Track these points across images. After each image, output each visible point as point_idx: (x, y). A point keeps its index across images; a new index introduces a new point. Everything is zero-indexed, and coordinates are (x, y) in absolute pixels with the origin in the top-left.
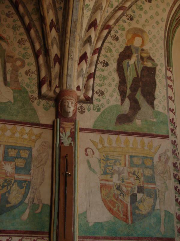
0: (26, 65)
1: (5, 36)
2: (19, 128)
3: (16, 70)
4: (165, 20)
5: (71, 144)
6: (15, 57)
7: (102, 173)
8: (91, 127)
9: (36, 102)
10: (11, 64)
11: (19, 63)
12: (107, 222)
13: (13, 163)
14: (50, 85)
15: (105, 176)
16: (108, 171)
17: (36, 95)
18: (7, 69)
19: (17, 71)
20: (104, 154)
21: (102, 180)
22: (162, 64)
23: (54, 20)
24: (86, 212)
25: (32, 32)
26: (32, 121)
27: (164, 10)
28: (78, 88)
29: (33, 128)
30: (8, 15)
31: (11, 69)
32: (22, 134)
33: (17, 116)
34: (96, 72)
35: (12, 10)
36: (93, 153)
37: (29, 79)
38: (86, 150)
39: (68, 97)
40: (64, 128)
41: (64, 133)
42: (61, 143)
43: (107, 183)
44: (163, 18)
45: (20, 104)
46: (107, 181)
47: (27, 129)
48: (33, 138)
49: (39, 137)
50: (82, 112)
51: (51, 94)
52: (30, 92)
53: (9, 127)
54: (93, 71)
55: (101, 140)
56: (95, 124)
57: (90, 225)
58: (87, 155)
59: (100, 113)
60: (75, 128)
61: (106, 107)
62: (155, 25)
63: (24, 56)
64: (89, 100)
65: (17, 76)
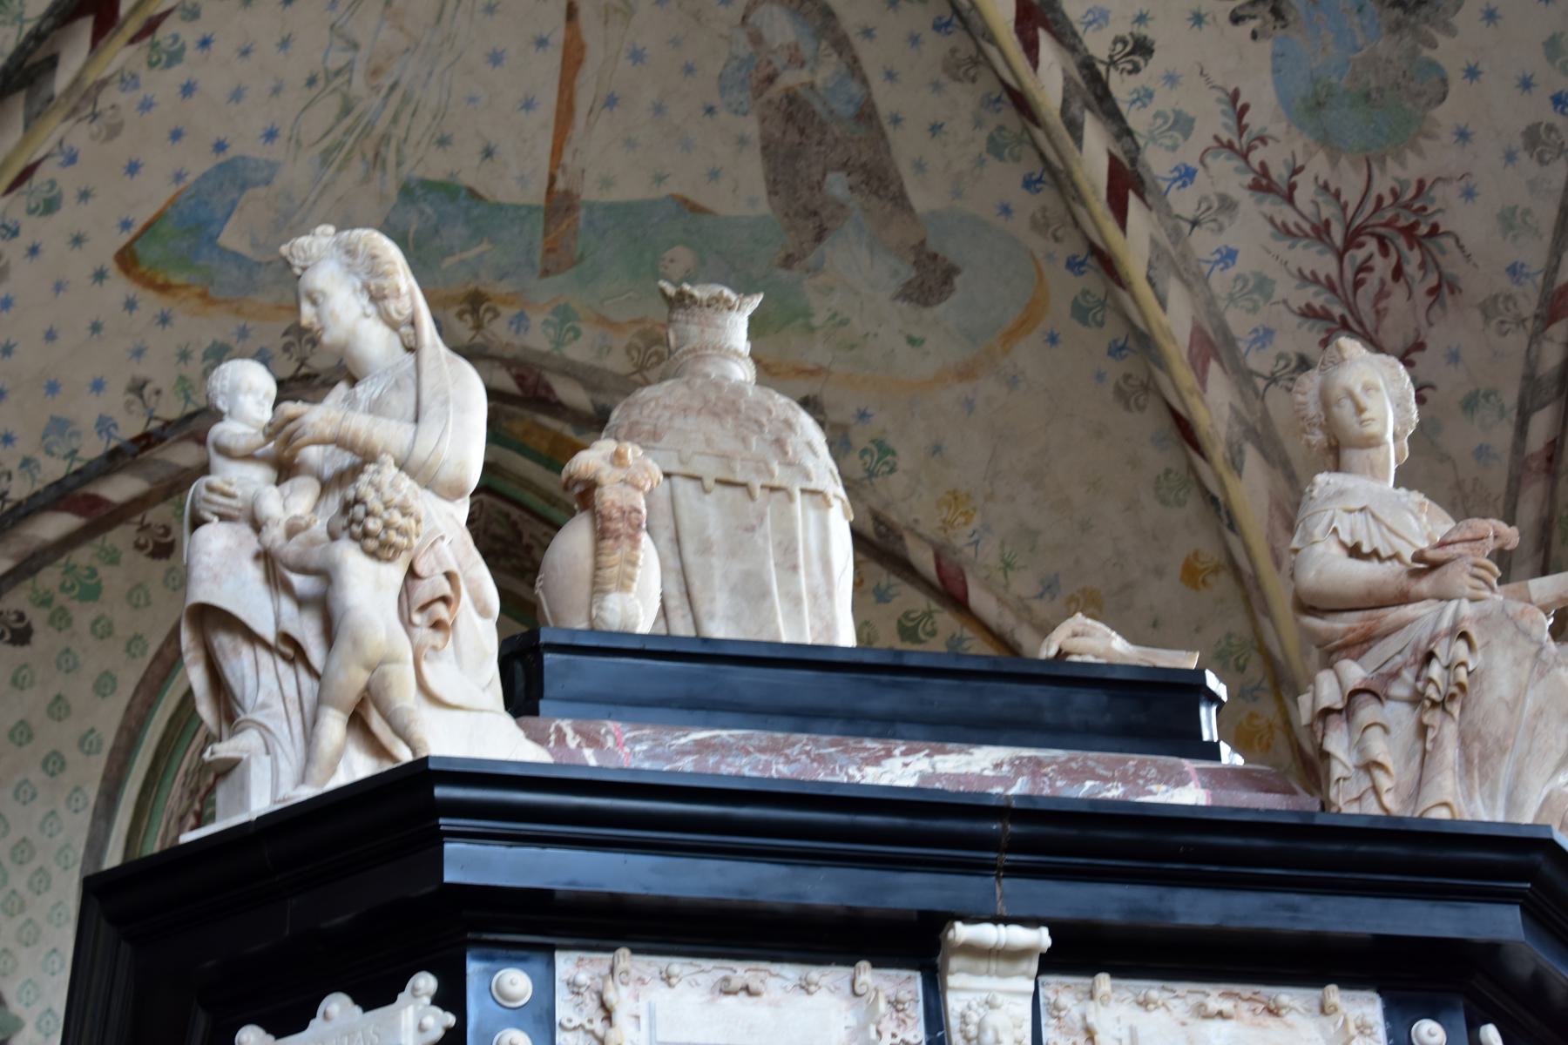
4: (109, 740)
22: (49, 1017)
27: (105, 684)
44: (92, 731)
62: (36, 776)
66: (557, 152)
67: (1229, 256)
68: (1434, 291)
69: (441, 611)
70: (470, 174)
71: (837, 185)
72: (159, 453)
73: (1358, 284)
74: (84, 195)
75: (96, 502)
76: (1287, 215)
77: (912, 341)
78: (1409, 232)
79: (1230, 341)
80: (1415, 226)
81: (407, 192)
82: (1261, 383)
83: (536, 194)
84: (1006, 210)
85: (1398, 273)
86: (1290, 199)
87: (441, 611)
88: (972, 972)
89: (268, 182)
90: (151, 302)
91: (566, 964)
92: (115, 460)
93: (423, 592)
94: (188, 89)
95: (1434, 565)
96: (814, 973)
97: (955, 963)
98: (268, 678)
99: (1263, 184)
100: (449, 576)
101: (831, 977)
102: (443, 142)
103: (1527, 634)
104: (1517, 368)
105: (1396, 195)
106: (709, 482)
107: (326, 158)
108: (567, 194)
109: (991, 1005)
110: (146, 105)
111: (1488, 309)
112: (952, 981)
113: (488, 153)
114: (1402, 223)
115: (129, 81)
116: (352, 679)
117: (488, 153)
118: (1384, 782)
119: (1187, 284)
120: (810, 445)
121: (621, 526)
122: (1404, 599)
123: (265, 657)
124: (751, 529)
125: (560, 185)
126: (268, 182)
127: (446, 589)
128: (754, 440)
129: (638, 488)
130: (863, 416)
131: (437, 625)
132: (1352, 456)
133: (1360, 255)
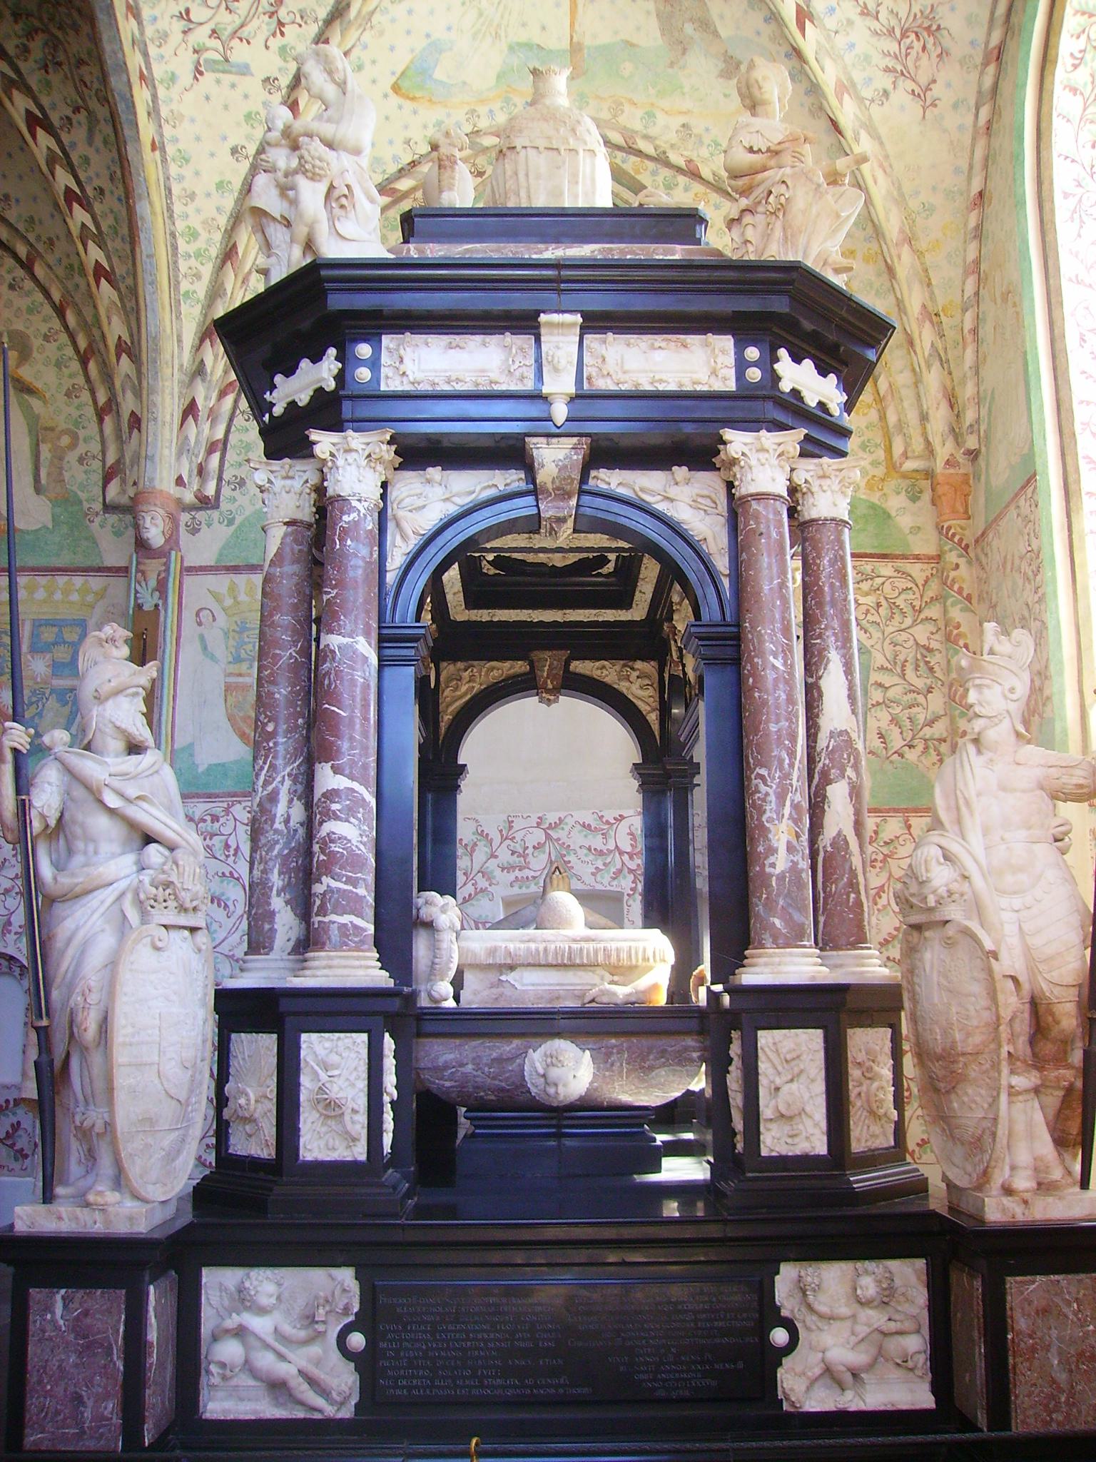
0: (81, 441)
1: (38, 385)
2: (62, 580)
3: (59, 456)
5: (156, 606)
6: (60, 429)
7: (231, 659)
8: (213, 564)
9: (98, 520)
10: (49, 445)
11: (65, 441)
12: (236, 762)
13: (49, 656)
14: (123, 481)
15: (236, 666)
16: (243, 655)
17: (98, 506)
18: (42, 458)
19: (61, 459)
20: (235, 619)
21: (230, 674)
23: (126, 337)
24: (191, 745)
25: (92, 366)
26: (88, 563)
28: (180, 481)
29: (90, 579)
30: (46, 338)
31: (49, 455)
32: (66, 592)
33: (58, 555)
34: (231, 437)
35: (56, 324)
36: (214, 620)
37: (85, 472)
38: (198, 615)
39: (145, 508)
40: (143, 573)
41: (143, 584)
42: (139, 607)
43: (240, 679)
45: (65, 529)
46: (240, 675)
47: (78, 581)
48: (90, 598)
49: (101, 595)
50: (194, 531)
51: (124, 500)
52: (87, 501)
53: (42, 581)
54: (220, 434)
55: (233, 589)
56: (221, 555)
57: (200, 770)
58: (200, 624)
59: (233, 528)
60: (167, 570)
61: (247, 513)
63: (77, 424)
64: (205, 503)
65: (61, 468)
66: (572, 25)
67: (852, 46)
68: (940, 56)
69: (344, 201)
70: (537, 38)
71: (689, 29)
72: (418, 169)
73: (907, 55)
74: (374, 62)
75: (394, 191)
76: (875, 25)
77: (725, 96)
78: (928, 29)
79: (853, 84)
80: (930, 26)
81: (511, 49)
82: (867, 103)
83: (565, 44)
84: (758, 33)
85: (924, 48)
86: (877, 19)
87: (344, 201)
88: (551, 334)
89: (451, 49)
90: (408, 105)
91: (386, 340)
92: (401, 173)
93: (336, 194)
94: (410, 12)
95: (777, 153)
96: (488, 338)
97: (543, 331)
98: (279, 235)
99: (865, 12)
100: (348, 186)
101: (494, 339)
102: (524, 25)
103: (811, 180)
104: (975, 88)
105: (922, 12)
106: (541, 149)
107: (474, 37)
108: (579, 43)
109: (558, 348)
110: (393, 21)
111: (962, 62)
112: (543, 339)
113: (544, 28)
114: (926, 25)
115: (386, 11)
116: (302, 231)
117: (544, 28)
118: (751, 249)
119: (834, 60)
120: (588, 131)
121: (447, 163)
122: (765, 169)
123: (279, 226)
124: (558, 168)
125: (575, 39)
126: (451, 49)
127: (346, 192)
128: (562, 130)
129: (455, 146)
130: (707, 130)
131: (342, 207)
132: (759, 109)
133: (908, 41)
